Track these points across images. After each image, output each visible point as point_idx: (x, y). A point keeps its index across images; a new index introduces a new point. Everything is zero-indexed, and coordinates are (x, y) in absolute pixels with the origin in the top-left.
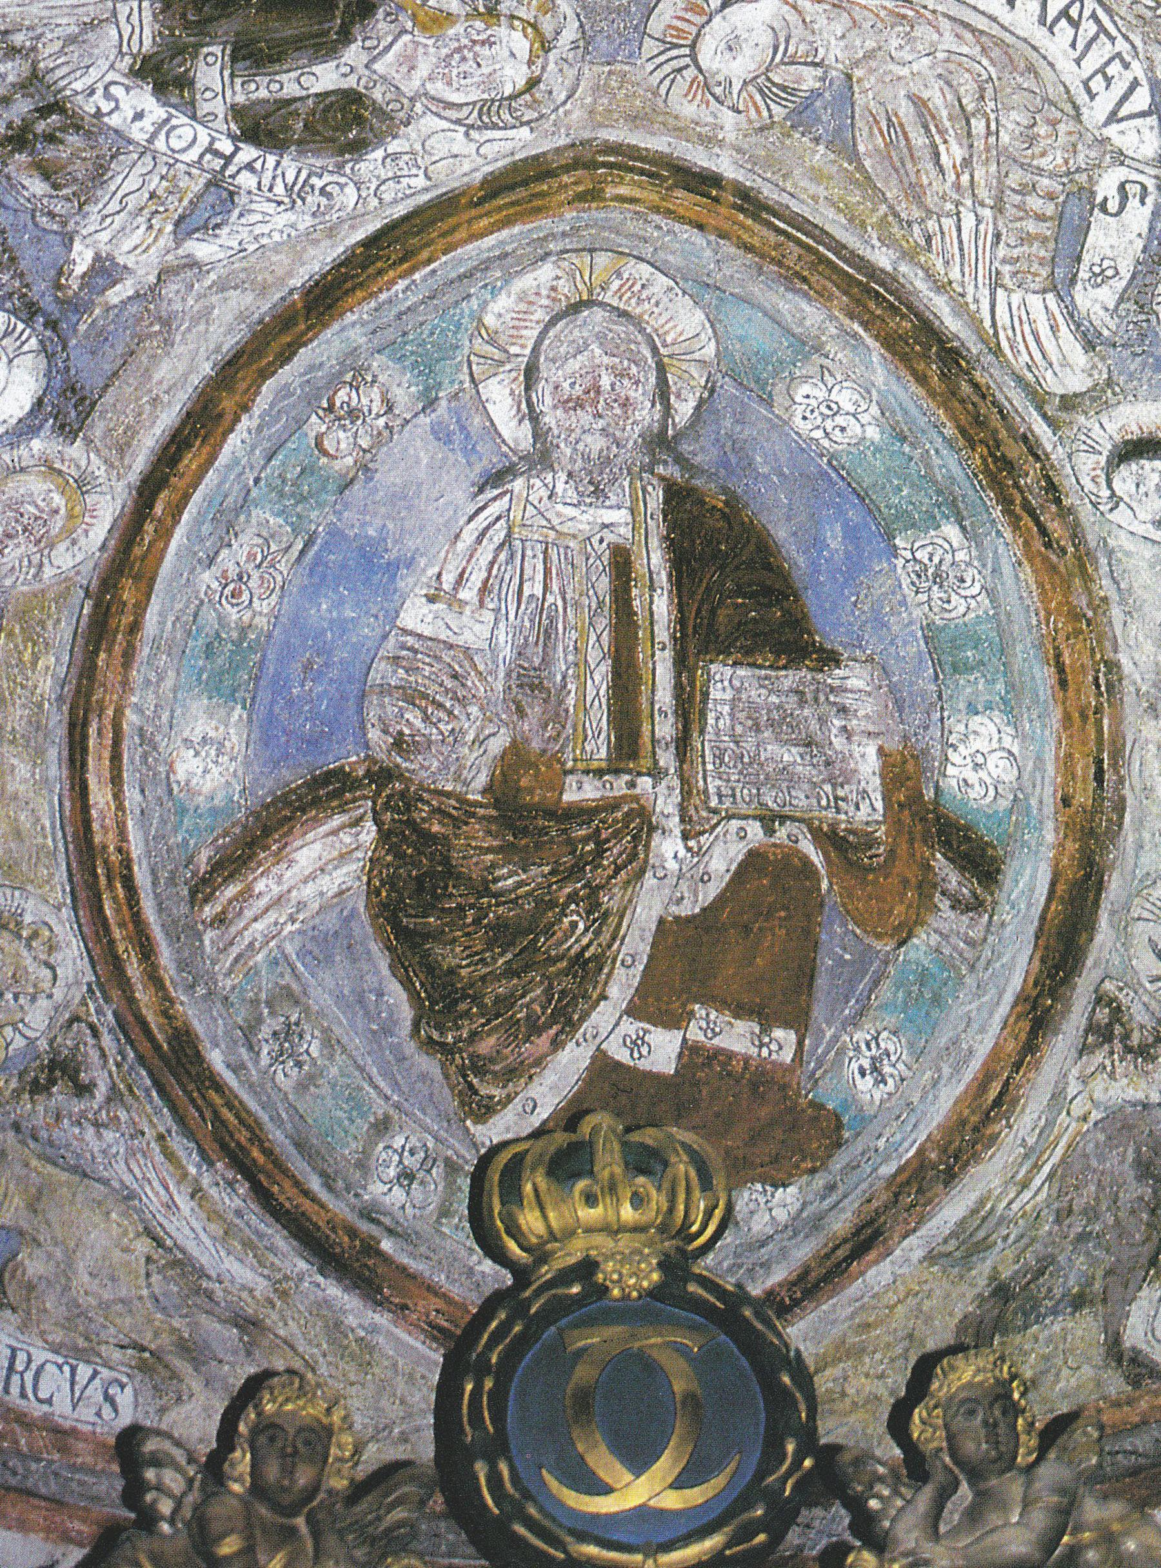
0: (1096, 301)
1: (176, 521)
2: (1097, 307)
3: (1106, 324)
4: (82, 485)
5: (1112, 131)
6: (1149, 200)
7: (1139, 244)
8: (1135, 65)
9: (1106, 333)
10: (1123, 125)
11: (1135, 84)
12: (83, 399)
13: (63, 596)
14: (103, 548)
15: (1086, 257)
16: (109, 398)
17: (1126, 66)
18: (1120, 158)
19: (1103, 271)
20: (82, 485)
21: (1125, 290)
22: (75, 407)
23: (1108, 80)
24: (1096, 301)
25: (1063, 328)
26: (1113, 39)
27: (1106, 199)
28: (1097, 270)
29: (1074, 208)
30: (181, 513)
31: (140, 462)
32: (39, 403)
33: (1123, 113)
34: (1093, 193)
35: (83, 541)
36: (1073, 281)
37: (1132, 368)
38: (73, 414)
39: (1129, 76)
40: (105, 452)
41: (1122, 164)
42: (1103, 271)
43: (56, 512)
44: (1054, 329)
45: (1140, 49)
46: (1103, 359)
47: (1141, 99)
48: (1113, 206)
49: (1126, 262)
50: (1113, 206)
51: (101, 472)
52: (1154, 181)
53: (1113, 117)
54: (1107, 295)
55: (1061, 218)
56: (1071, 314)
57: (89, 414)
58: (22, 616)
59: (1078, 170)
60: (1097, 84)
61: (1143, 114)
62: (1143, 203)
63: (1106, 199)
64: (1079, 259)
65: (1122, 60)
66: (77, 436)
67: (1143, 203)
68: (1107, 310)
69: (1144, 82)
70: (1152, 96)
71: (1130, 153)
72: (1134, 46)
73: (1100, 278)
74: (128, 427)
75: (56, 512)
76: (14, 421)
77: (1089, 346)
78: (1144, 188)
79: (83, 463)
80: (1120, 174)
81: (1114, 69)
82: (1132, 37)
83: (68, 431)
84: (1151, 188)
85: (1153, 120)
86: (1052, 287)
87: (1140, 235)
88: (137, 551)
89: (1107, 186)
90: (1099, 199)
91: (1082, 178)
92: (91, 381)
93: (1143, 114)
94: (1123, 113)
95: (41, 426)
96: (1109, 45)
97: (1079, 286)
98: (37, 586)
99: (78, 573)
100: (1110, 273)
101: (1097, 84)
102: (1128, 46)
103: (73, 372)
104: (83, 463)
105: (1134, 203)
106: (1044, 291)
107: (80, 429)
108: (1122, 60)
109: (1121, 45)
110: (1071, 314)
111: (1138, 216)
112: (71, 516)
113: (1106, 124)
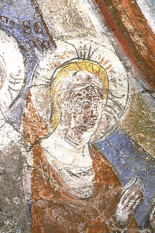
1: (145, 22)
4: (84, 57)
12: (36, 25)
13: (141, 104)
14: (127, 69)
16: (45, 12)
20: (84, 57)
22: (37, 32)
30: (142, 16)
31: (94, 20)
32: (22, 48)
35: (116, 76)
38: (40, 36)
40: (74, 34)
43: (89, 78)
51: (84, 42)
57: (47, 29)
58: (137, 128)
66: (53, 42)
74: (70, 14)
75: (89, 78)
76: (22, 66)
79: (71, 48)
83: (48, 44)
88: (144, 53)
92: (29, 15)
95: (35, 57)
98: (127, 112)
99: (133, 90)
103: (16, 21)
104: (71, 48)
107: (51, 38)
112: (97, 73)
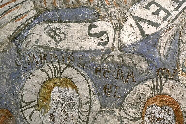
0: (40, 35)
2: (37, 37)
3: (29, 44)
5: (130, 20)
6: (101, 47)
7: (77, 48)
8: (166, 23)
9: (24, 45)
10: (134, 25)
11: (156, 25)
15: (63, 25)
17: (165, 19)
18: (118, 28)
19: (58, 35)
21: (51, 48)
23: (157, 13)
24: (40, 35)
25: (19, 23)
26: (177, 9)
27: (96, 27)
28: (58, 32)
29: (88, 13)
33: (142, 24)
34: (97, 20)
36: (48, 21)
37: (8, 62)
39: (160, 21)
41: (115, 30)
42: (58, 35)
44: (17, 18)
45: (173, 23)
46: (8, 47)
47: (149, 30)
48: (94, 31)
49: (65, 45)
50: (94, 31)
52: (111, 46)
53: (138, 20)
54: (45, 40)
55: (80, 8)
56: (29, 25)
59: (106, 10)
60: (154, 8)
61: (142, 32)
62: (98, 44)
63: (96, 27)
64: (61, 21)
65: (167, 17)
67: (98, 44)
68: (37, 41)
69: (158, 29)
70: (153, 34)
71: (122, 32)
72: (174, 20)
73: (53, 34)
77: (13, 38)
78: (106, 43)
80: (110, 30)
81: (162, 14)
82: (179, 18)
84: (107, 46)
85: (140, 37)
86: (40, 12)
87: (81, 47)
89: (102, 25)
90: (95, 24)
91: (103, 13)
93: (142, 32)
94: (141, 23)
96: (173, 9)
97: (45, 25)
100: (58, 38)
101: (154, 8)
102: (174, 17)
105: (98, 41)
106: (36, 8)
108: (167, 17)
109: (174, 14)
110: (29, 25)
111: (91, 44)
113: (134, 18)
